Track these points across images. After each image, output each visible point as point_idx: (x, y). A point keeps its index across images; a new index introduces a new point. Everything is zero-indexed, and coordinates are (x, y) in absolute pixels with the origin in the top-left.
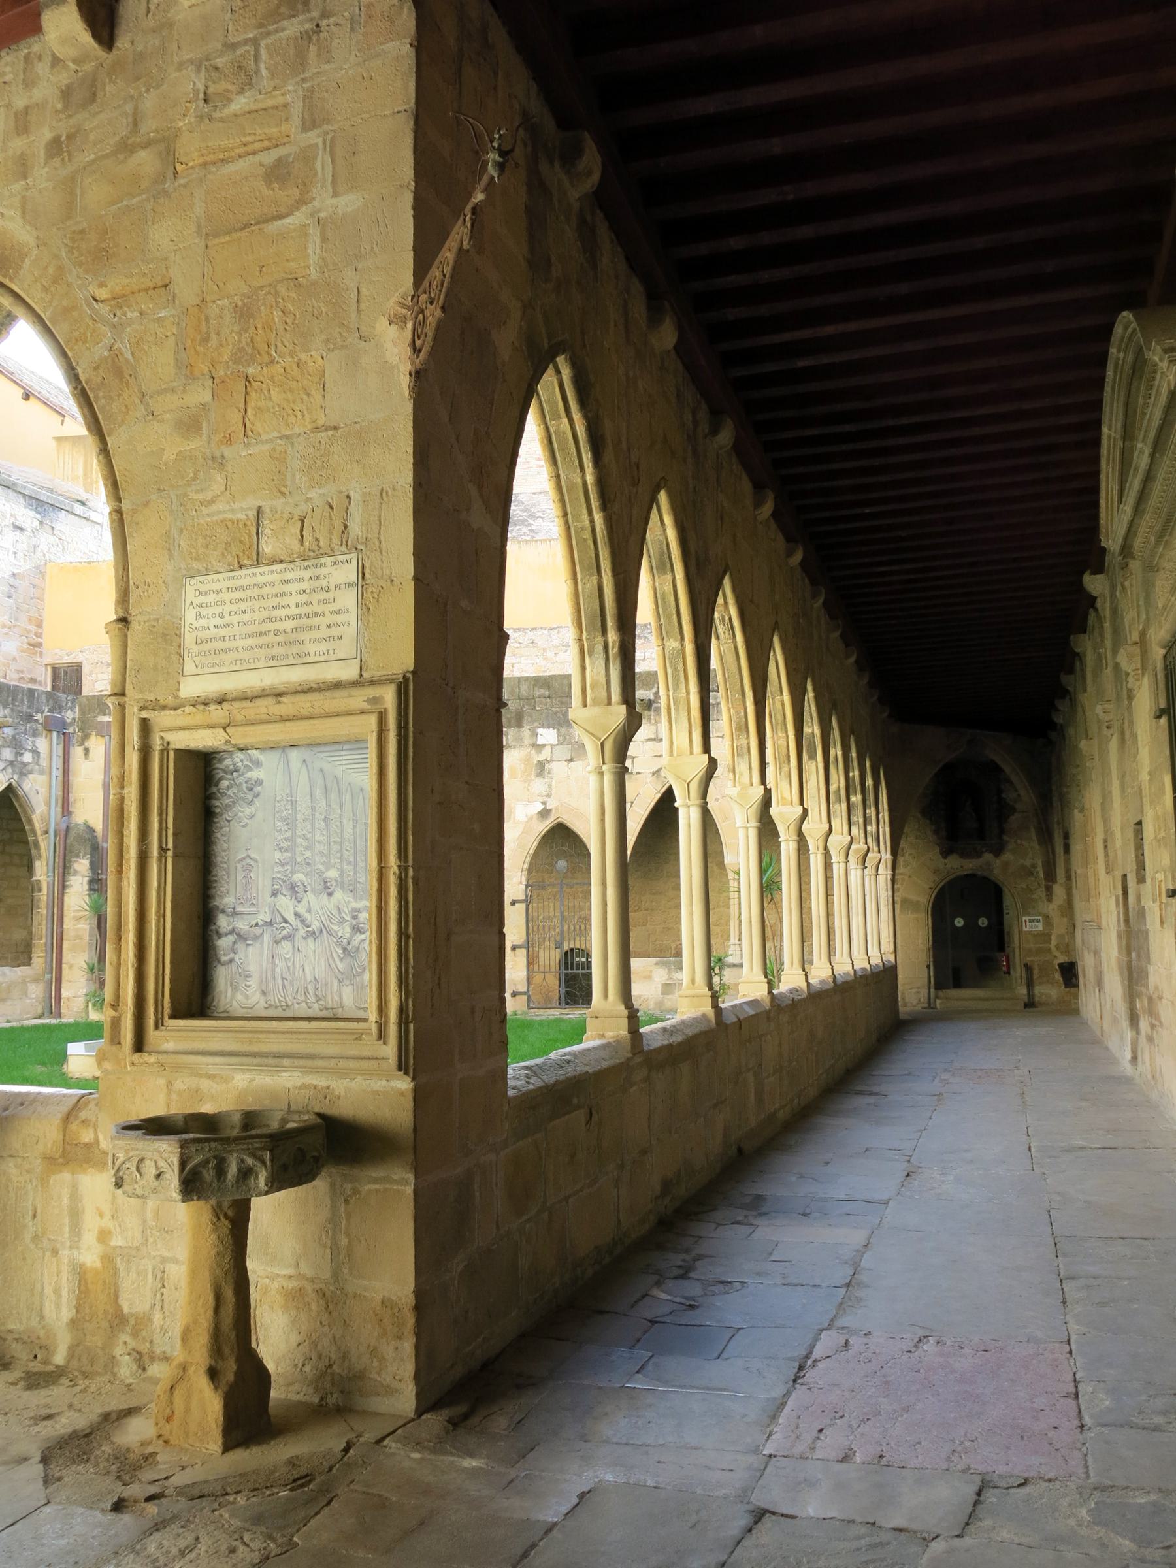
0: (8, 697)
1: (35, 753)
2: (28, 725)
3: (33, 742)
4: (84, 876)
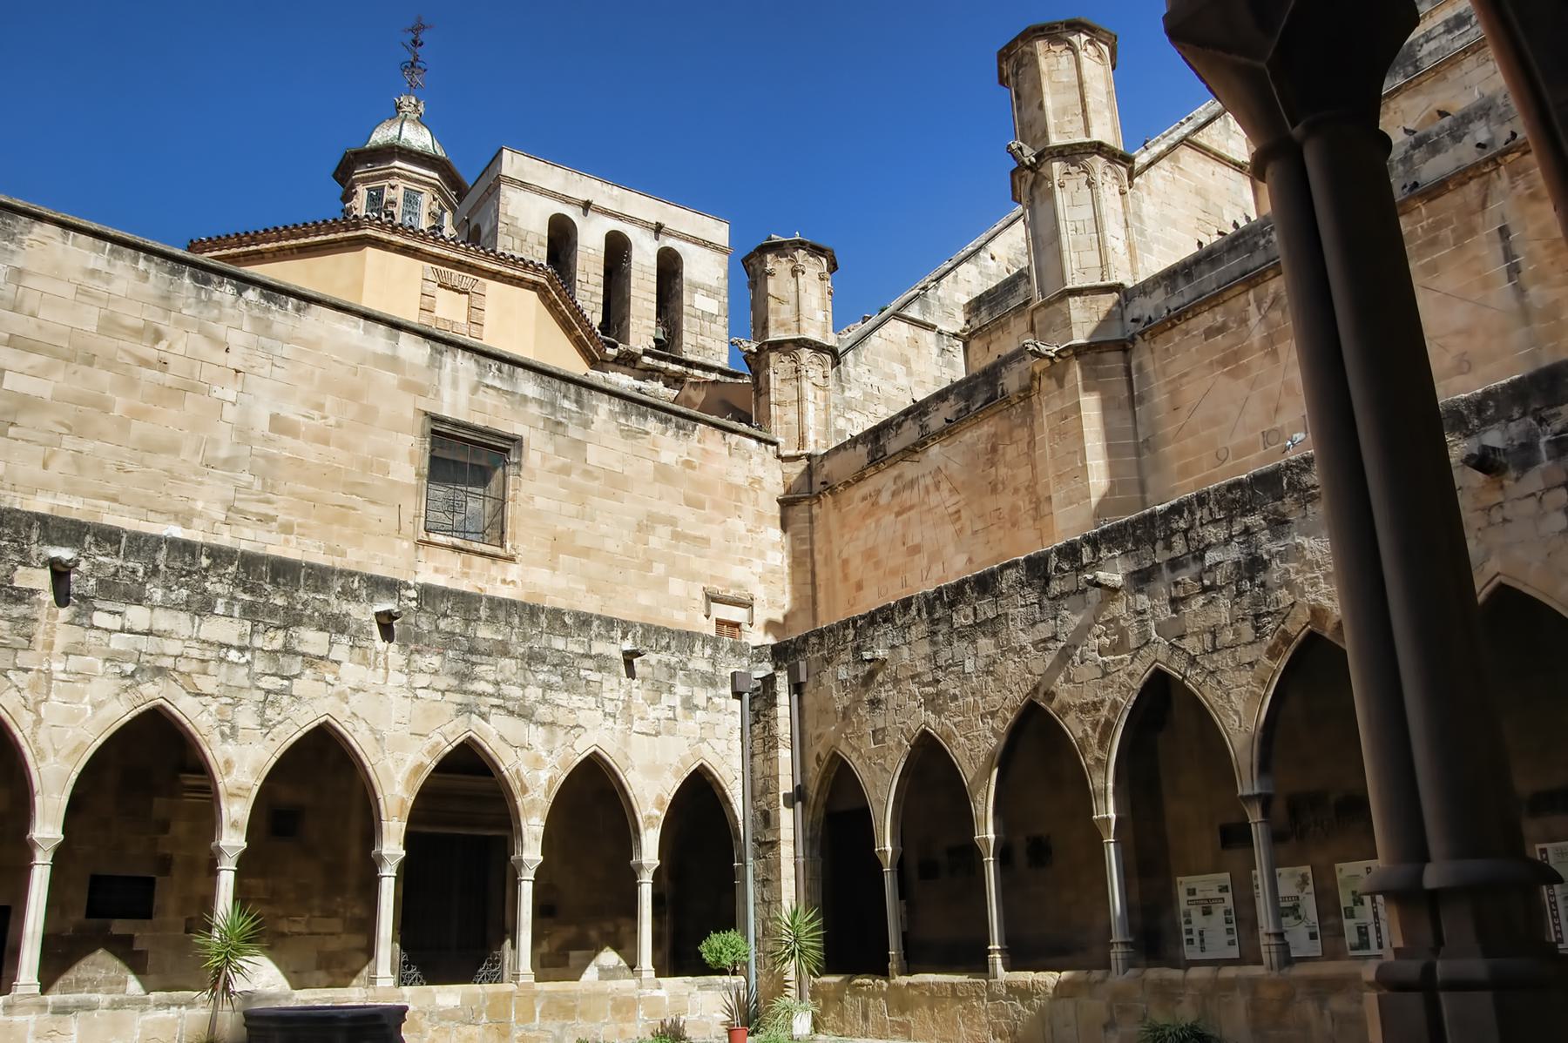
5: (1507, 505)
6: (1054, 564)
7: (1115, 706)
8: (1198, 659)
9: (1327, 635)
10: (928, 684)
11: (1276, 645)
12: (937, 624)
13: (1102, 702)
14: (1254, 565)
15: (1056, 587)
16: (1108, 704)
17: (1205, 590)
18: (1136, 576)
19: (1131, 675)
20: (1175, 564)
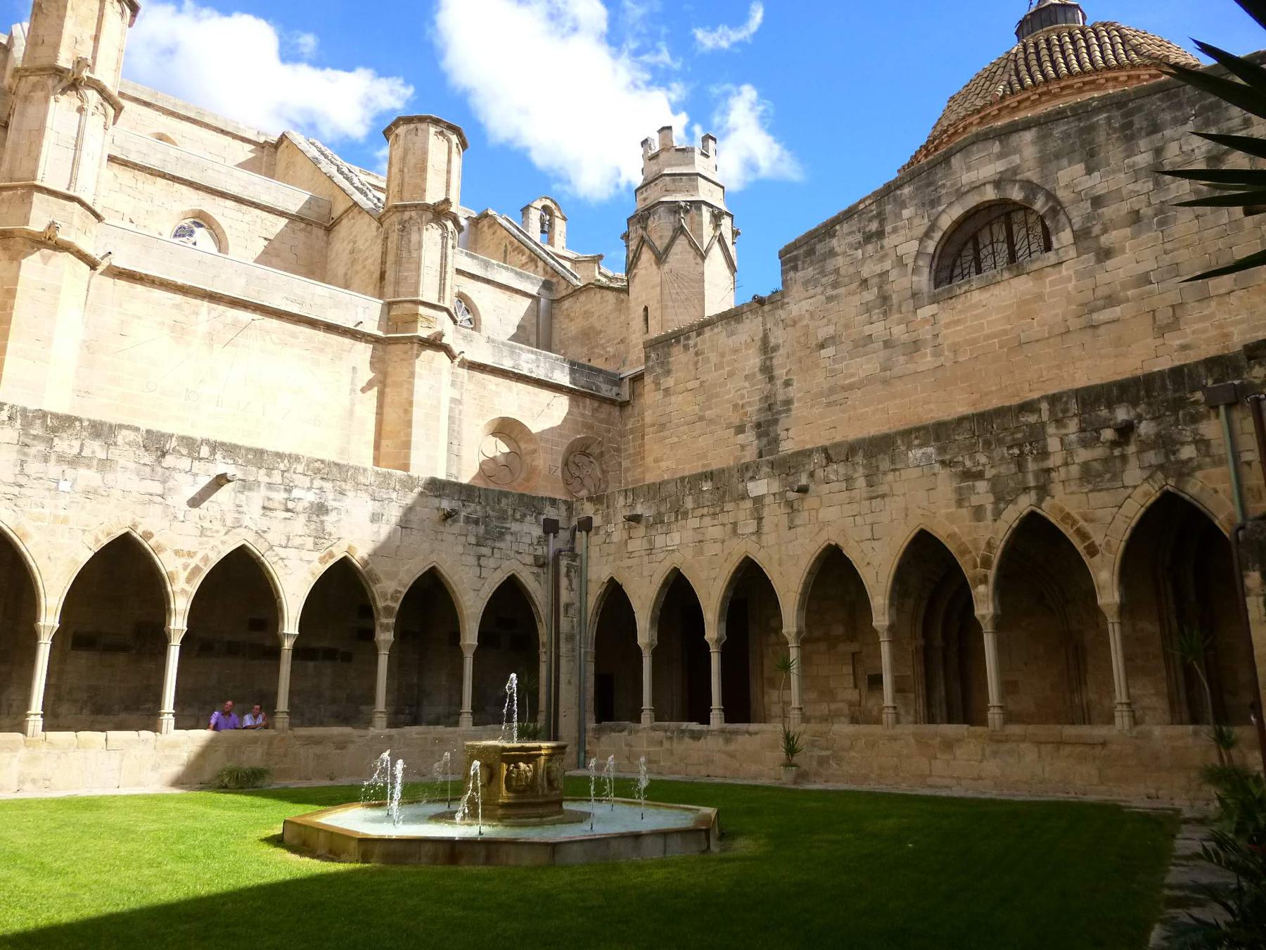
0: (1138, 391)
1: (1202, 443)
3: (1195, 432)
4: (1258, 595)
6: (173, 446)
7: (206, 559)
8: (274, 548)
9: (354, 561)
10: (10, 485)
11: (325, 557)
12: (34, 439)
13: (195, 553)
14: (320, 509)
15: (169, 461)
16: (199, 556)
17: (288, 510)
18: (240, 482)
19: (223, 543)
20: (270, 486)
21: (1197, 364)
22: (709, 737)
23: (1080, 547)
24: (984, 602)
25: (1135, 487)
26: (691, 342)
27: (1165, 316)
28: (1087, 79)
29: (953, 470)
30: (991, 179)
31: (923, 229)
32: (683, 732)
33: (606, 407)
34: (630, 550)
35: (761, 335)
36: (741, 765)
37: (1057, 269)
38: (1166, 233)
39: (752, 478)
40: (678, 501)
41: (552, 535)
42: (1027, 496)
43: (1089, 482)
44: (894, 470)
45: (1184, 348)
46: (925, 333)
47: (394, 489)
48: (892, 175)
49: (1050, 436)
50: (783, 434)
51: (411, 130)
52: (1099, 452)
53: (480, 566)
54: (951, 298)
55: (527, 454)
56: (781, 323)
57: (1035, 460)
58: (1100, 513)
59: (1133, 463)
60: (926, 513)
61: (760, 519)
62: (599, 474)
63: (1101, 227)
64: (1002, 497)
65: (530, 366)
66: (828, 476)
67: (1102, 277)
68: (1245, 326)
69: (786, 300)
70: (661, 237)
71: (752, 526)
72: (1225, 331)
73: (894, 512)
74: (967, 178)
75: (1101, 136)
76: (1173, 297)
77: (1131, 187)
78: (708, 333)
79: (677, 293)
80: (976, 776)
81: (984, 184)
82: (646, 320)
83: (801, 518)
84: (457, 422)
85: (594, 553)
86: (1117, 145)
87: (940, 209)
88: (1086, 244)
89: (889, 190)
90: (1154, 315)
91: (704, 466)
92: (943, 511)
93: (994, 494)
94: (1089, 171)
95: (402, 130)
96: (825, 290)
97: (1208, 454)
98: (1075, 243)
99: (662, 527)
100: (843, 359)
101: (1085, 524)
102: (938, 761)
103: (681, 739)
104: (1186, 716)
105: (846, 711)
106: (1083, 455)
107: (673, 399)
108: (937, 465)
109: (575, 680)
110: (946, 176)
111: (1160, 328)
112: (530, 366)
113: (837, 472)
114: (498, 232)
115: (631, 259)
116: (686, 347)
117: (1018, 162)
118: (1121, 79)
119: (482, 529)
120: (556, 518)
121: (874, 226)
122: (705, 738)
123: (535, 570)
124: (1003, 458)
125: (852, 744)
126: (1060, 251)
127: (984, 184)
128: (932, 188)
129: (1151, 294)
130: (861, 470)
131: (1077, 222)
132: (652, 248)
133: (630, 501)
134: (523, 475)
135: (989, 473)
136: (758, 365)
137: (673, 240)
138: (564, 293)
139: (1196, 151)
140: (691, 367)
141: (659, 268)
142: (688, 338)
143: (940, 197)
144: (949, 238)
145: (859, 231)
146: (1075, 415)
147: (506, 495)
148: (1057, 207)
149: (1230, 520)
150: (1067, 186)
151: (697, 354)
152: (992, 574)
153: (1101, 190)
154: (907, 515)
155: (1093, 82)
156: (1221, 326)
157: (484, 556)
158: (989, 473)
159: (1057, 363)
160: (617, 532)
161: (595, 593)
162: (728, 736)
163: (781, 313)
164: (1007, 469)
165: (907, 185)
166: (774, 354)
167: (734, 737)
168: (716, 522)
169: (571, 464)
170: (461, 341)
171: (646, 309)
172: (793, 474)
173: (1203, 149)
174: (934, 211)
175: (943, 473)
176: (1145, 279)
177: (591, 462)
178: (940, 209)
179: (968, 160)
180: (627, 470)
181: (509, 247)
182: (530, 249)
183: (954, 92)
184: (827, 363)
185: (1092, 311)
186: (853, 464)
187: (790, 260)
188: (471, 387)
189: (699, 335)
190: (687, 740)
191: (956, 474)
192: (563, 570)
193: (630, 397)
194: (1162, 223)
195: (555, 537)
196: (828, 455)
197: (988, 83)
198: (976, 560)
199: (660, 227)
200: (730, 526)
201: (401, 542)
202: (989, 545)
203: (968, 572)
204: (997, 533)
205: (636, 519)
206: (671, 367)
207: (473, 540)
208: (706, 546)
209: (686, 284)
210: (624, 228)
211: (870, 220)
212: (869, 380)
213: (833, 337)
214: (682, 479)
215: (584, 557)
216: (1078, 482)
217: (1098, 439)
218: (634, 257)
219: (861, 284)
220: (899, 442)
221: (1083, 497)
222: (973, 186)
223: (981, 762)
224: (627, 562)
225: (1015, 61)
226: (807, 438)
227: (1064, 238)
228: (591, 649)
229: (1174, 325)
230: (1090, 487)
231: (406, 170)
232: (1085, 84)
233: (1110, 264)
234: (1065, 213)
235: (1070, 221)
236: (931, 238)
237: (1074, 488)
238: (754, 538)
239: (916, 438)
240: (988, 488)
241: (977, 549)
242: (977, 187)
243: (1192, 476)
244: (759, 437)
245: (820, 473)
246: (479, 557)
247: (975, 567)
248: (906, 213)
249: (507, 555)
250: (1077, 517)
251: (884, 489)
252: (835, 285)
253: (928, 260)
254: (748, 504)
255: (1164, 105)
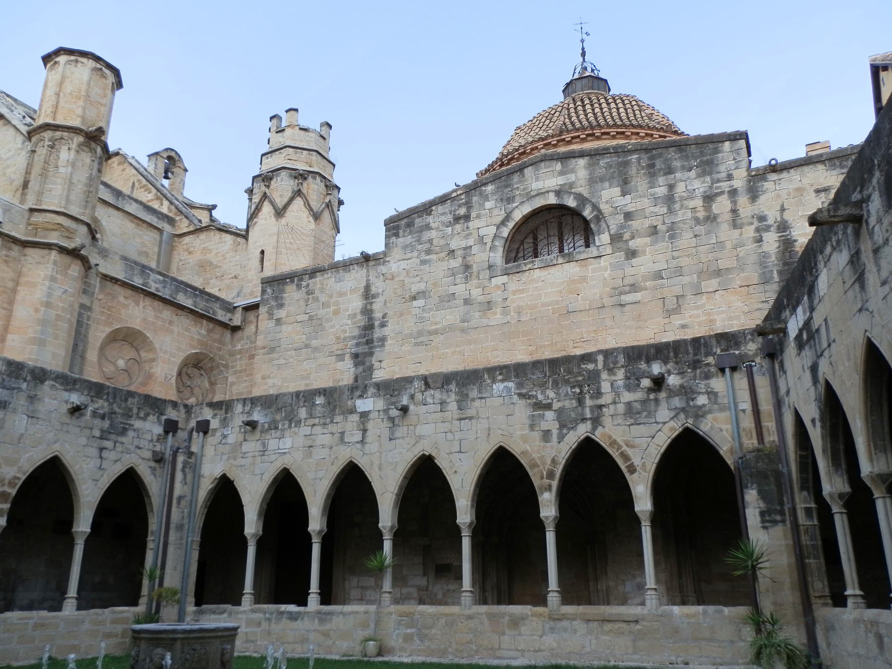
0: (669, 353)
1: (712, 394)
2: (698, 371)
3: (707, 386)
5: (70, 426)
21: (710, 337)
22: (306, 618)
23: (623, 467)
24: (548, 506)
25: (664, 423)
26: (304, 284)
27: (671, 303)
28: (619, 130)
29: (528, 401)
30: (553, 189)
31: (500, 218)
32: (282, 613)
33: (219, 329)
34: (244, 451)
35: (364, 284)
36: (334, 643)
37: (598, 260)
38: (676, 244)
39: (361, 397)
40: (293, 410)
41: (171, 434)
42: (585, 425)
43: (631, 418)
44: (481, 398)
45: (684, 326)
46: (497, 296)
47: (25, 380)
48: (469, 178)
49: (604, 381)
50: (376, 365)
51: (71, 61)
52: (639, 395)
53: (101, 457)
54: (518, 273)
55: (145, 362)
56: (382, 276)
57: (591, 398)
58: (638, 441)
59: (664, 405)
60: (504, 433)
61: (365, 431)
62: (207, 385)
63: (630, 234)
64: (565, 424)
65: (157, 286)
66: (425, 399)
67: (629, 271)
68: (724, 316)
69: (387, 259)
70: (281, 196)
71: (358, 436)
72: (711, 317)
73: (479, 431)
74: (536, 186)
75: (633, 170)
76: (678, 290)
77: (652, 209)
78: (319, 278)
79: (291, 243)
80: (537, 648)
81: (548, 192)
82: (262, 261)
83: (401, 432)
84: (84, 326)
85: (209, 451)
86: (644, 178)
87: (515, 205)
88: (619, 245)
89: (473, 188)
90: (664, 301)
91: (306, 385)
92: (519, 433)
93: (559, 422)
94: (624, 194)
95: (62, 59)
96: (420, 254)
97: (716, 403)
98: (611, 244)
99: (275, 433)
100: (431, 310)
101: (627, 449)
102: (506, 636)
103: (278, 620)
104: (678, 600)
105: (415, 595)
106: (627, 397)
107: (284, 328)
108: (516, 397)
109: (180, 567)
110: (520, 182)
111: (667, 311)
112: (157, 286)
113: (433, 396)
114: (127, 170)
115: (253, 210)
116: (299, 287)
117: (574, 179)
118: (641, 134)
119: (106, 424)
120: (176, 419)
121: (462, 211)
122: (302, 619)
123: (153, 464)
124: (567, 394)
125: (434, 623)
126: (600, 248)
127: (548, 192)
128: (509, 189)
129: (662, 287)
130: (453, 397)
131: (614, 229)
132: (272, 203)
133: (247, 408)
134: (140, 379)
135: (556, 405)
136: (360, 307)
137: (291, 200)
138: (185, 230)
139: (697, 190)
140: (302, 303)
141: (277, 220)
142: (301, 280)
143: (514, 196)
144: (519, 228)
145: (451, 214)
146: (623, 366)
147: (131, 394)
148: (599, 217)
149: (732, 451)
150: (607, 202)
151: (308, 293)
152: (555, 484)
153: (630, 208)
154: (489, 435)
155: (623, 133)
156: (708, 314)
157: (106, 449)
158: (556, 405)
159: (594, 328)
160: (234, 434)
161: (206, 486)
162: (322, 617)
163: (383, 269)
164: (570, 404)
165: (490, 184)
166: (374, 300)
167: (329, 617)
168: (325, 431)
169: (184, 375)
170: (97, 256)
171: (262, 252)
172: (396, 396)
173: (701, 190)
174: (510, 206)
175: (521, 403)
176: (658, 275)
177: (202, 375)
178: (515, 205)
179: (537, 172)
180: (233, 384)
181: (137, 184)
182: (158, 190)
183: (520, 124)
184: (416, 311)
185: (621, 294)
186: (447, 392)
187: (394, 228)
188: (101, 296)
189: (311, 278)
190: (285, 621)
191: (530, 404)
192: (179, 466)
193: (242, 323)
194: (672, 237)
195: (173, 436)
196: (427, 382)
197: (548, 121)
198: (542, 473)
199: (282, 188)
200: (337, 436)
201: (26, 430)
202: (553, 461)
203: (536, 482)
204: (560, 452)
205: (252, 425)
206: (284, 302)
207: (97, 433)
208: (314, 451)
209: (299, 237)
210: (249, 184)
211: (460, 206)
212: (451, 328)
213: (424, 292)
214: (298, 394)
215: (199, 455)
216: (622, 416)
217: (638, 385)
218: (256, 208)
219: (449, 254)
220: (486, 376)
221: (627, 428)
222: (540, 192)
223: (541, 637)
224: (240, 461)
225: (568, 109)
226: (397, 369)
227: (603, 239)
228: (197, 538)
229: (677, 310)
230: (632, 421)
231: (62, 95)
232: (618, 133)
233: (635, 261)
234: (605, 221)
235: (608, 227)
236: (506, 226)
237: (620, 421)
238: (359, 446)
239: (500, 374)
240: (555, 418)
241: (544, 464)
242: (540, 194)
243: (705, 418)
244: (356, 365)
245: (419, 396)
246: (101, 449)
247: (542, 478)
248: (488, 205)
249: (128, 449)
250: (621, 443)
251: (470, 412)
252: (428, 252)
253: (502, 242)
254: (355, 418)
255: (676, 156)
